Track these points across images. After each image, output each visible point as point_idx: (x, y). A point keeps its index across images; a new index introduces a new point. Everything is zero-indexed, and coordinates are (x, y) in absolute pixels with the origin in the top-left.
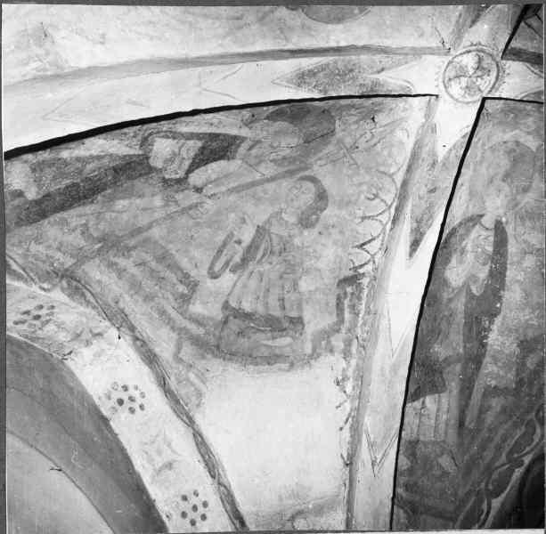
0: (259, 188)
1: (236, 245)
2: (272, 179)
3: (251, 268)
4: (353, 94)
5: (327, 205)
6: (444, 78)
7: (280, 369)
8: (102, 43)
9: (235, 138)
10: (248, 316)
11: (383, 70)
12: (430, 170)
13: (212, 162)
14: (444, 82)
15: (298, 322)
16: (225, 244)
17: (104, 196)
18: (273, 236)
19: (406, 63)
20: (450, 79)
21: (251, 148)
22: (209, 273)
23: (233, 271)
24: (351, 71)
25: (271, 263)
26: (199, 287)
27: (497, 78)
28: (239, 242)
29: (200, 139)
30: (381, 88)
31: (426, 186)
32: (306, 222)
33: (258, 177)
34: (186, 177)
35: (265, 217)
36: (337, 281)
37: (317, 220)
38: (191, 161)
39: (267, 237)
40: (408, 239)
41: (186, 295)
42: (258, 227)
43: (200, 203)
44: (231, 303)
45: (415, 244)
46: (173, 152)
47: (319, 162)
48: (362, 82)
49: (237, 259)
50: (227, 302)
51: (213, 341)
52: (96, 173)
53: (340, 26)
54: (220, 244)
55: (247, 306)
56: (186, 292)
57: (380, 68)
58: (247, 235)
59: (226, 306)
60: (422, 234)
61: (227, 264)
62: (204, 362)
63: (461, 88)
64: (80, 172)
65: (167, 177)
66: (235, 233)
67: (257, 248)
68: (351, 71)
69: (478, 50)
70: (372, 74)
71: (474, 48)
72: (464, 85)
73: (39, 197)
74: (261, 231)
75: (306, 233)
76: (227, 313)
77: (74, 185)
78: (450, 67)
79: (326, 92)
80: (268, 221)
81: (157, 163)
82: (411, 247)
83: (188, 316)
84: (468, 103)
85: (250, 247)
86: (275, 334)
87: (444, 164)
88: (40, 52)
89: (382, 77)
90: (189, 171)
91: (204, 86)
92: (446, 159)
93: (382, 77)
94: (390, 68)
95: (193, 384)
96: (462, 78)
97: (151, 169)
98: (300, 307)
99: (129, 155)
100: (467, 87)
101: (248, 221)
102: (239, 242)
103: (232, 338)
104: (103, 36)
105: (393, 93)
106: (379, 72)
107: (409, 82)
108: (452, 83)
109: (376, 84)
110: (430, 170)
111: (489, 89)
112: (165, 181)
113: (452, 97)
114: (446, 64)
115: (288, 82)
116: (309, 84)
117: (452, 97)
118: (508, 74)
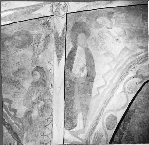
6: (67, 6)
11: (86, 6)
14: (67, 5)
24: (96, 5)
27: (52, 10)
57: (87, 7)
69: (61, 16)
70: (89, 5)
71: (63, 17)
72: (61, 6)
94: (84, 7)
96: (62, 7)
100: (60, 5)
106: (87, 5)
111: (53, 6)
118: (50, 12)
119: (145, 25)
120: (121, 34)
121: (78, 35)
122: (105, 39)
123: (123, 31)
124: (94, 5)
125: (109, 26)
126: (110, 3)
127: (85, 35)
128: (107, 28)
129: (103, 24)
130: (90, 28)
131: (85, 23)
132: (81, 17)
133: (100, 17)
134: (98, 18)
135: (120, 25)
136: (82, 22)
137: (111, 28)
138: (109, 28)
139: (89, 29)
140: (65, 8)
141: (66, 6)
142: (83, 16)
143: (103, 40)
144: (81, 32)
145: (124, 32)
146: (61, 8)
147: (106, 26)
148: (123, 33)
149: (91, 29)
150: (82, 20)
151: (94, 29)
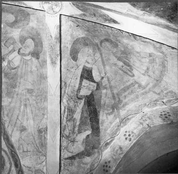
0: (104, 59)
1: (124, 67)
2: (101, 54)
3: (131, 64)
4: (59, 46)
5: (110, 39)
6: (53, 14)
7: (167, 64)
8: (44, 115)
9: (83, 69)
10: (148, 69)
11: (51, 36)
12: (87, 16)
13: (92, 75)
14: (55, 14)
15: (150, 55)
16: (123, 71)
17: (98, 108)
18: (121, 56)
19: (49, 28)
20: (54, 12)
21: (89, 63)
22: (132, 77)
23: (132, 70)
24: (51, 47)
25: (130, 58)
26: (137, 81)
28: (123, 66)
29: (82, 80)
30: (57, 36)
31: (93, 17)
32: (116, 46)
33: (100, 59)
34: (97, 83)
35: (114, 58)
36: (135, 40)
37: (115, 42)
38: (91, 82)
39: (122, 58)
40: (112, 24)
41: (139, 85)
42: (118, 60)
43: (107, 77)
44: (143, 73)
45: (115, 22)
46: (86, 88)
47: (95, 41)
48: (55, 43)
49: (128, 68)
50: (143, 74)
51: (155, 82)
52: (88, 112)
53: (43, 43)
54: (122, 72)
55: (145, 68)
56: (138, 85)
57: (50, 37)
58: (121, 64)
59: (144, 75)
60: (111, 19)
61: (130, 71)
62: (161, 86)
63: (57, 7)
64: (86, 118)
65: (95, 89)
66: (119, 67)
67: (125, 61)
68: (51, 47)
71: (41, 6)
72: (55, 7)
73: (91, 129)
74: (119, 59)
75: (119, 46)
76: (146, 75)
77: (90, 119)
78: (49, 13)
79: (58, 55)
80: (116, 57)
81: (89, 93)
82: (116, 23)
83: (146, 87)
84: (62, 5)
85: (124, 63)
86: (155, 61)
87: (85, 11)
88: (43, 133)
89: (53, 36)
90: (94, 82)
91: (53, 94)
92: (82, 10)
93: (53, 36)
95: (168, 93)
96: (53, 7)
97: (92, 95)
98: (146, 53)
99: (84, 102)
100: (56, 5)
101: (115, 63)
102: (123, 66)
103: (155, 75)
104: (43, 114)
105: (59, 32)
106: (52, 37)
107: (55, 27)
108: (55, 11)
109: (56, 38)
110: (87, 16)
112: (97, 89)
113: (60, 10)
114: (48, 14)
115: (54, 67)
116: (55, 60)
117: (60, 10)
119: (22, 90)
120: (11, 65)
121: (12, 14)
122: (5, 45)
123: (15, 67)
124: (52, 45)
125: (21, 51)
126: (51, 62)
127: (13, 21)
128: (20, 49)
129: (24, 45)
130: (20, 28)
131: (28, 24)
132: (36, 22)
133: (34, 43)
134: (33, 41)
135: (22, 64)
136: (29, 21)
137: (19, 53)
138: (19, 51)
139: (19, 27)
140: (52, 11)
141: (54, 13)
142: (37, 24)
143: (4, 42)
144: (16, 17)
145: (14, 67)
146: (52, 6)
147: (21, 48)
148: (12, 66)
149: (20, 30)
150: (32, 21)
151: (18, 33)
